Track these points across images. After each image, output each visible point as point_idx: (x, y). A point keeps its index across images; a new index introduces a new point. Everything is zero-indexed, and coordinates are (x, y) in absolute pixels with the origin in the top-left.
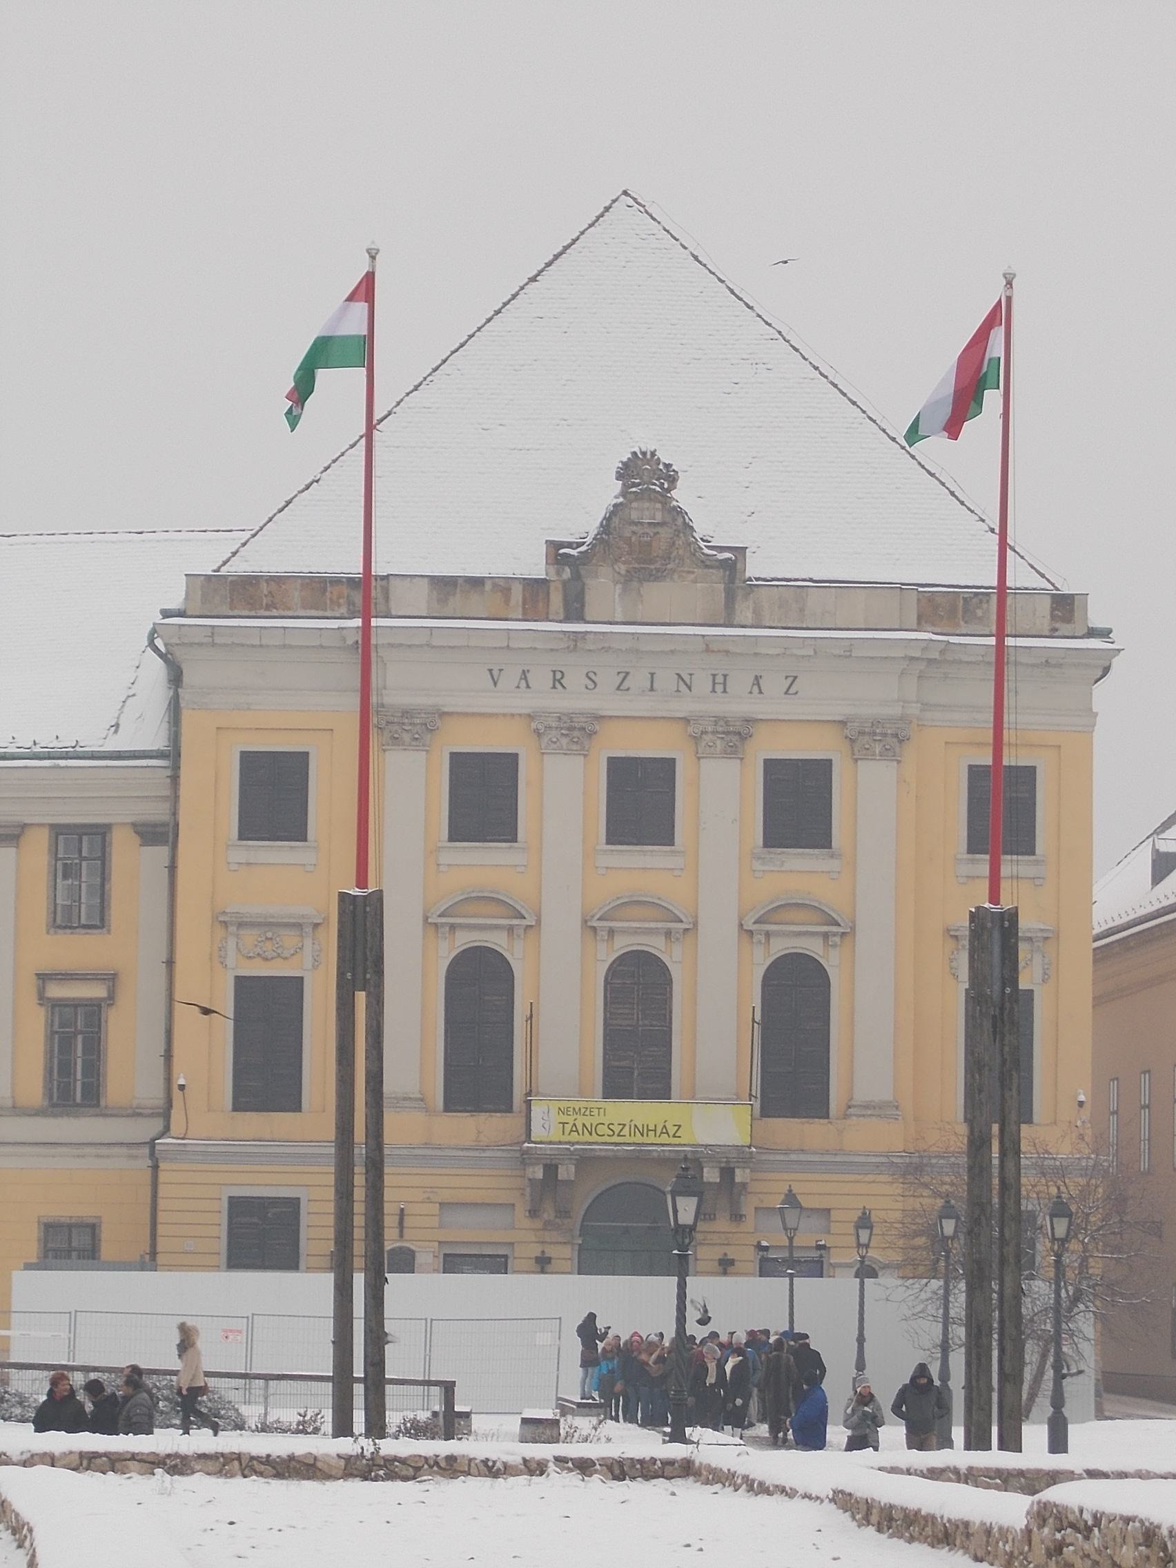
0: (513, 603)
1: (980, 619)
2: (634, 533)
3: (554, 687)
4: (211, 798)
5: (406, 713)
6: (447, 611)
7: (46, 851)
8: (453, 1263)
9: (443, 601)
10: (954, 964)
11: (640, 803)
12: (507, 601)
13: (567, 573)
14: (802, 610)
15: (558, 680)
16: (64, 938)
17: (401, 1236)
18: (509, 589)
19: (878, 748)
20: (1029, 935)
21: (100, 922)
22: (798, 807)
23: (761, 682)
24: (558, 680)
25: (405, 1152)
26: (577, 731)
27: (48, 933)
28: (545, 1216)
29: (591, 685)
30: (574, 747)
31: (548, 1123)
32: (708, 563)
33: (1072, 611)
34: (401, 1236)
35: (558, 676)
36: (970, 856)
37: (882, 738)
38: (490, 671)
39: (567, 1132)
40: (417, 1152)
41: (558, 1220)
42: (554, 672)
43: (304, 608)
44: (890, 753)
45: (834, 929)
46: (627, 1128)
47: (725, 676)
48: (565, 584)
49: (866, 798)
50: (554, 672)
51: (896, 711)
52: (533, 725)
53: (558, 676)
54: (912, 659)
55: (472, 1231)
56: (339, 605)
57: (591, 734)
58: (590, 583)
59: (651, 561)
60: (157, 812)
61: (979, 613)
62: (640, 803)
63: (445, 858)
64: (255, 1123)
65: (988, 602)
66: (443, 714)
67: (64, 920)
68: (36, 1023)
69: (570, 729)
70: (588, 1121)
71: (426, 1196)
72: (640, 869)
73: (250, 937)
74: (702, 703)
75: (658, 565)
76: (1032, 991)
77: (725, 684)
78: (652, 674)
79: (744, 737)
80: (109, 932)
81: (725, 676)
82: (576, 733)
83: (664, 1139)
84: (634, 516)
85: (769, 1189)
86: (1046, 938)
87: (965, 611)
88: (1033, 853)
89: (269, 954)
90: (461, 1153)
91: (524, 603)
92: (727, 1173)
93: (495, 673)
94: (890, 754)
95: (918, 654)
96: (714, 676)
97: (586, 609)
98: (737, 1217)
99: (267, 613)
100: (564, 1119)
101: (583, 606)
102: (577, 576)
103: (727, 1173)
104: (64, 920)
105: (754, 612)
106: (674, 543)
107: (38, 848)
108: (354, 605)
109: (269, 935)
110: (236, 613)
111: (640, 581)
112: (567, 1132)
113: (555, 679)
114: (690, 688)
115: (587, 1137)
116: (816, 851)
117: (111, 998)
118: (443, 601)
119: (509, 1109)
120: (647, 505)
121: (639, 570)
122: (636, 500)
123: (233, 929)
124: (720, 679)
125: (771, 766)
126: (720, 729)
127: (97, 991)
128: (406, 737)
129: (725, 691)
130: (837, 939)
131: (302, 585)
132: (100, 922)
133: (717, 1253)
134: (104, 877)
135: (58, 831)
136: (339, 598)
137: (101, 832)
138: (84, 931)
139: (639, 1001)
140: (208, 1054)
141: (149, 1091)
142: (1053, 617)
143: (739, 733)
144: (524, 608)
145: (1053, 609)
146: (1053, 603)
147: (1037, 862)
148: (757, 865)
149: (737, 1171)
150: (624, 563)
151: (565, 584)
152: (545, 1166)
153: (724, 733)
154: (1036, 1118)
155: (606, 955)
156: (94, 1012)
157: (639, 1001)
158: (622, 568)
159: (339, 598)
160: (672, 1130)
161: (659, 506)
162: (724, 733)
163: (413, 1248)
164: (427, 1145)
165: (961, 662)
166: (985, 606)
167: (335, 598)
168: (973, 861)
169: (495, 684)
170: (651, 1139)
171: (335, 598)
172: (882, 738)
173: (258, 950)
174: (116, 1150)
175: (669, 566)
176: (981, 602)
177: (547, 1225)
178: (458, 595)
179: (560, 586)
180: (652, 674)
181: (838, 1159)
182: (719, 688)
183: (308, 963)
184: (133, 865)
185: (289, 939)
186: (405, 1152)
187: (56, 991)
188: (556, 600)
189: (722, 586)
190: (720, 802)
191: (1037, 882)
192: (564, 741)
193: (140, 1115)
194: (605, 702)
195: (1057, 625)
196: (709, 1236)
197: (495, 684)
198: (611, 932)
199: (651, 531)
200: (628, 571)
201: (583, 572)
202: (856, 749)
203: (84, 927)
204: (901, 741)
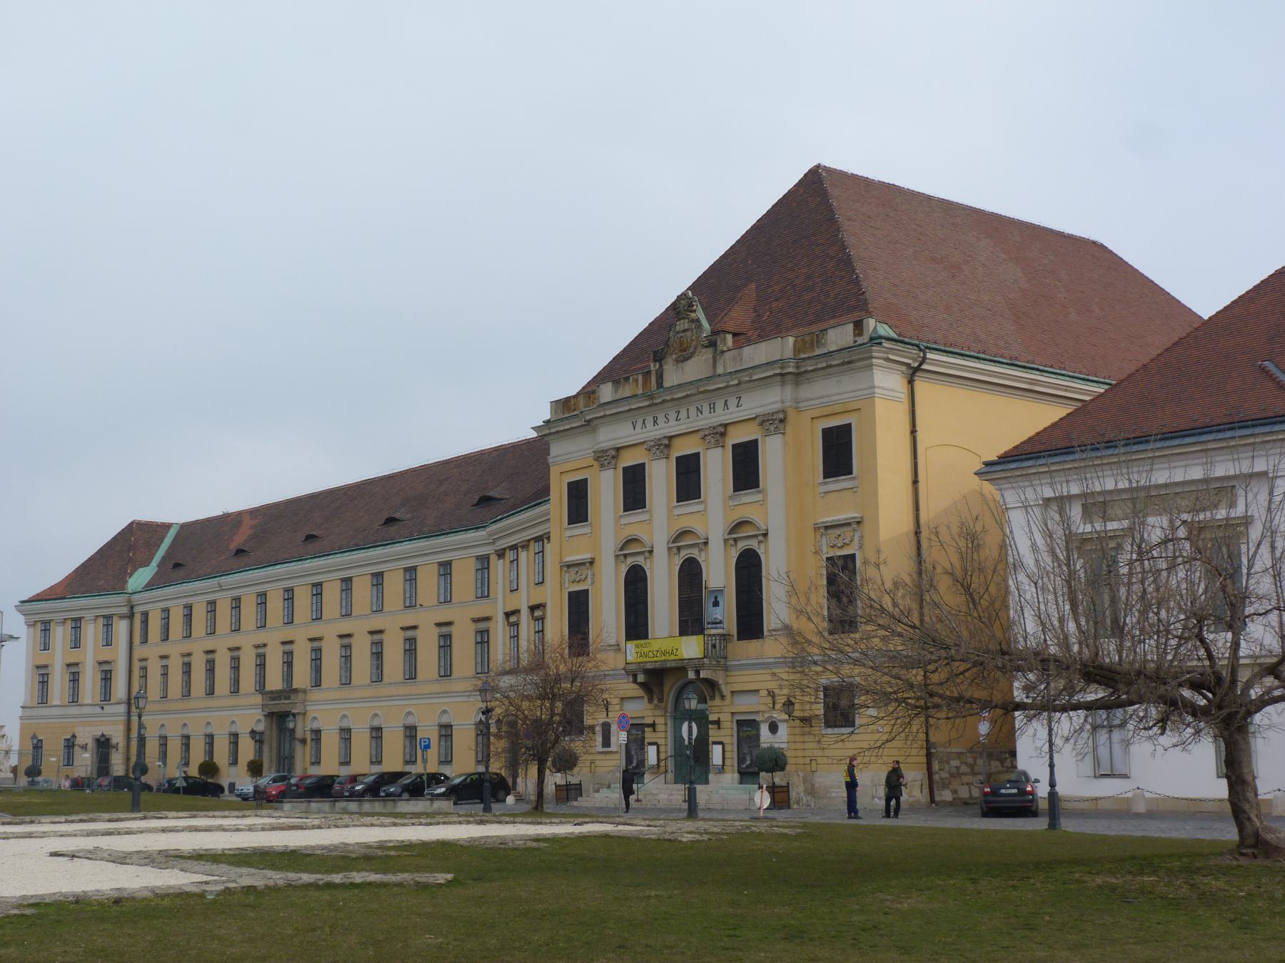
9: (616, 392)
11: (688, 480)
19: (772, 428)
37: (775, 422)
49: (772, 456)
51: (777, 406)
58: (665, 367)
62: (688, 480)
79: (723, 435)
95: (778, 371)
102: (661, 366)
118: (616, 392)
130: (761, 538)
142: (855, 335)
147: (853, 478)
148: (731, 503)
165: (806, 372)
172: (775, 422)
198: (679, 548)
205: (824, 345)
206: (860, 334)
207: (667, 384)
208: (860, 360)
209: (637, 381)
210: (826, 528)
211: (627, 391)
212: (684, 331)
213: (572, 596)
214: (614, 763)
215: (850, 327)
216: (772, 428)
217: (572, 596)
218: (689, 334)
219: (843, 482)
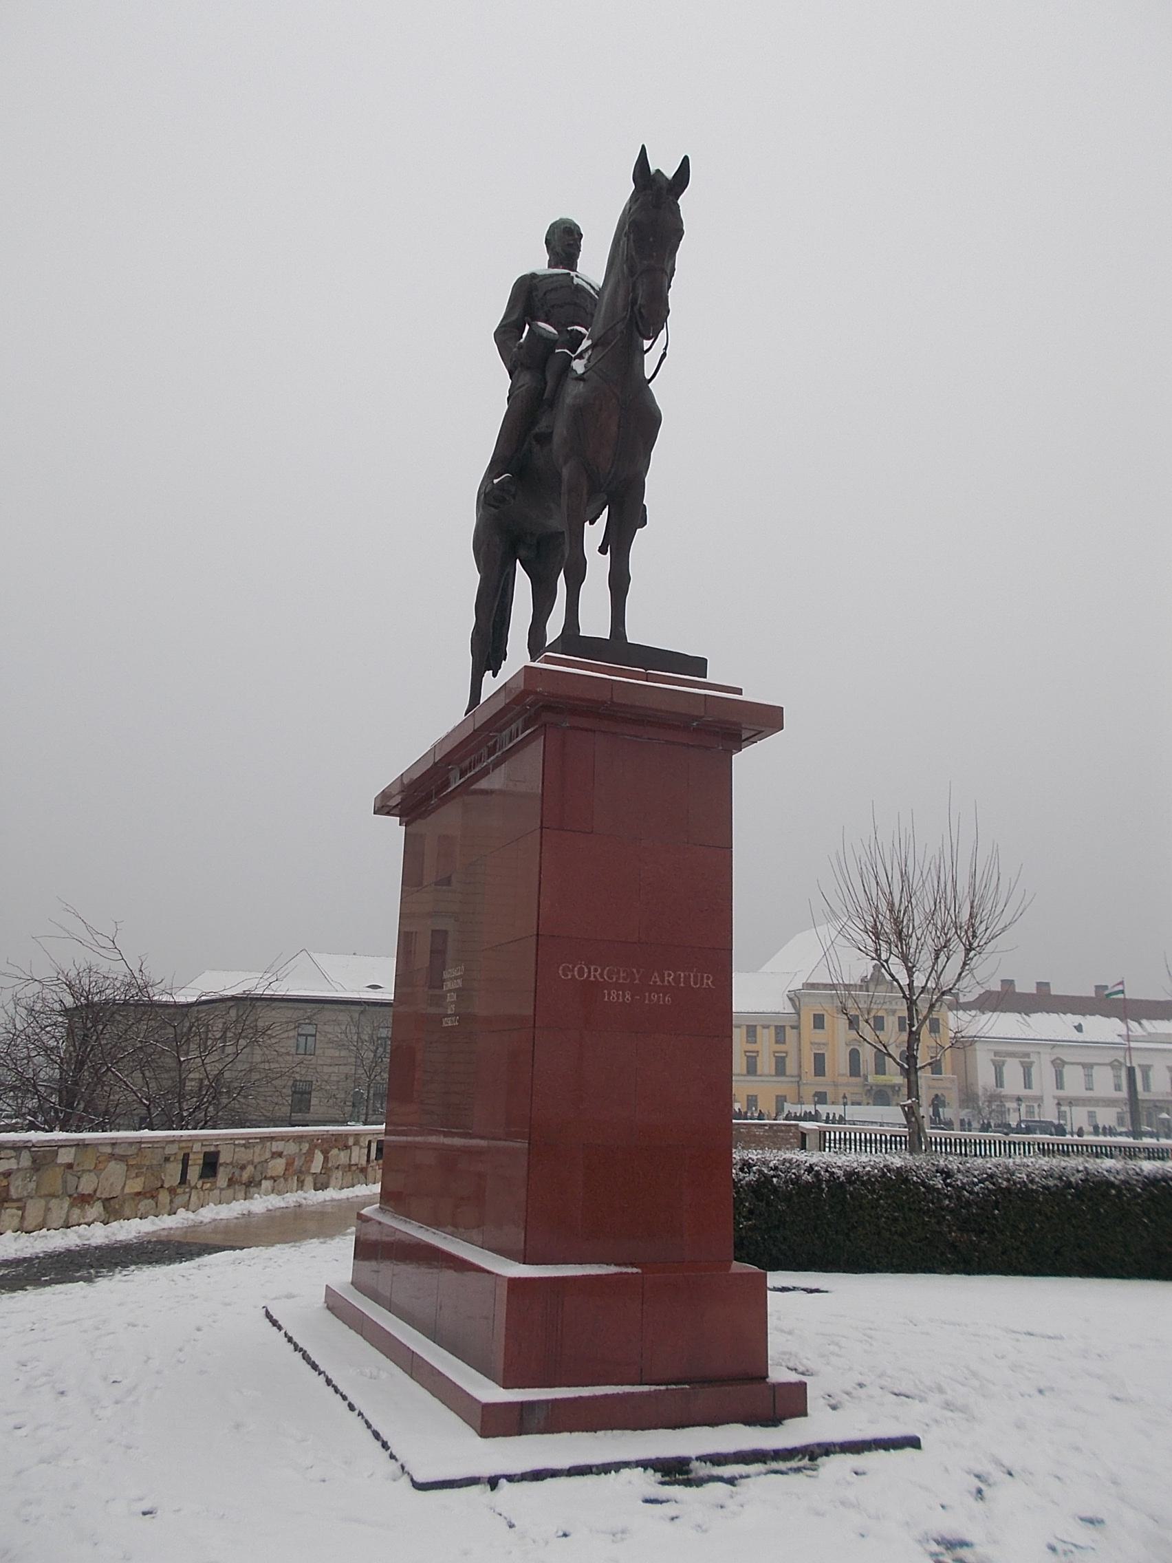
4: (807, 1021)
8: (853, 1104)
21: (784, 1043)
31: (870, 1079)
55: (857, 1098)
67: (777, 1042)
68: (773, 1060)
104: (777, 1042)
107: (773, 1029)
132: (784, 1043)
135: (776, 1027)
137: (784, 1027)
140: (809, 1066)
141: (795, 1072)
156: (783, 1058)
184: (790, 1034)
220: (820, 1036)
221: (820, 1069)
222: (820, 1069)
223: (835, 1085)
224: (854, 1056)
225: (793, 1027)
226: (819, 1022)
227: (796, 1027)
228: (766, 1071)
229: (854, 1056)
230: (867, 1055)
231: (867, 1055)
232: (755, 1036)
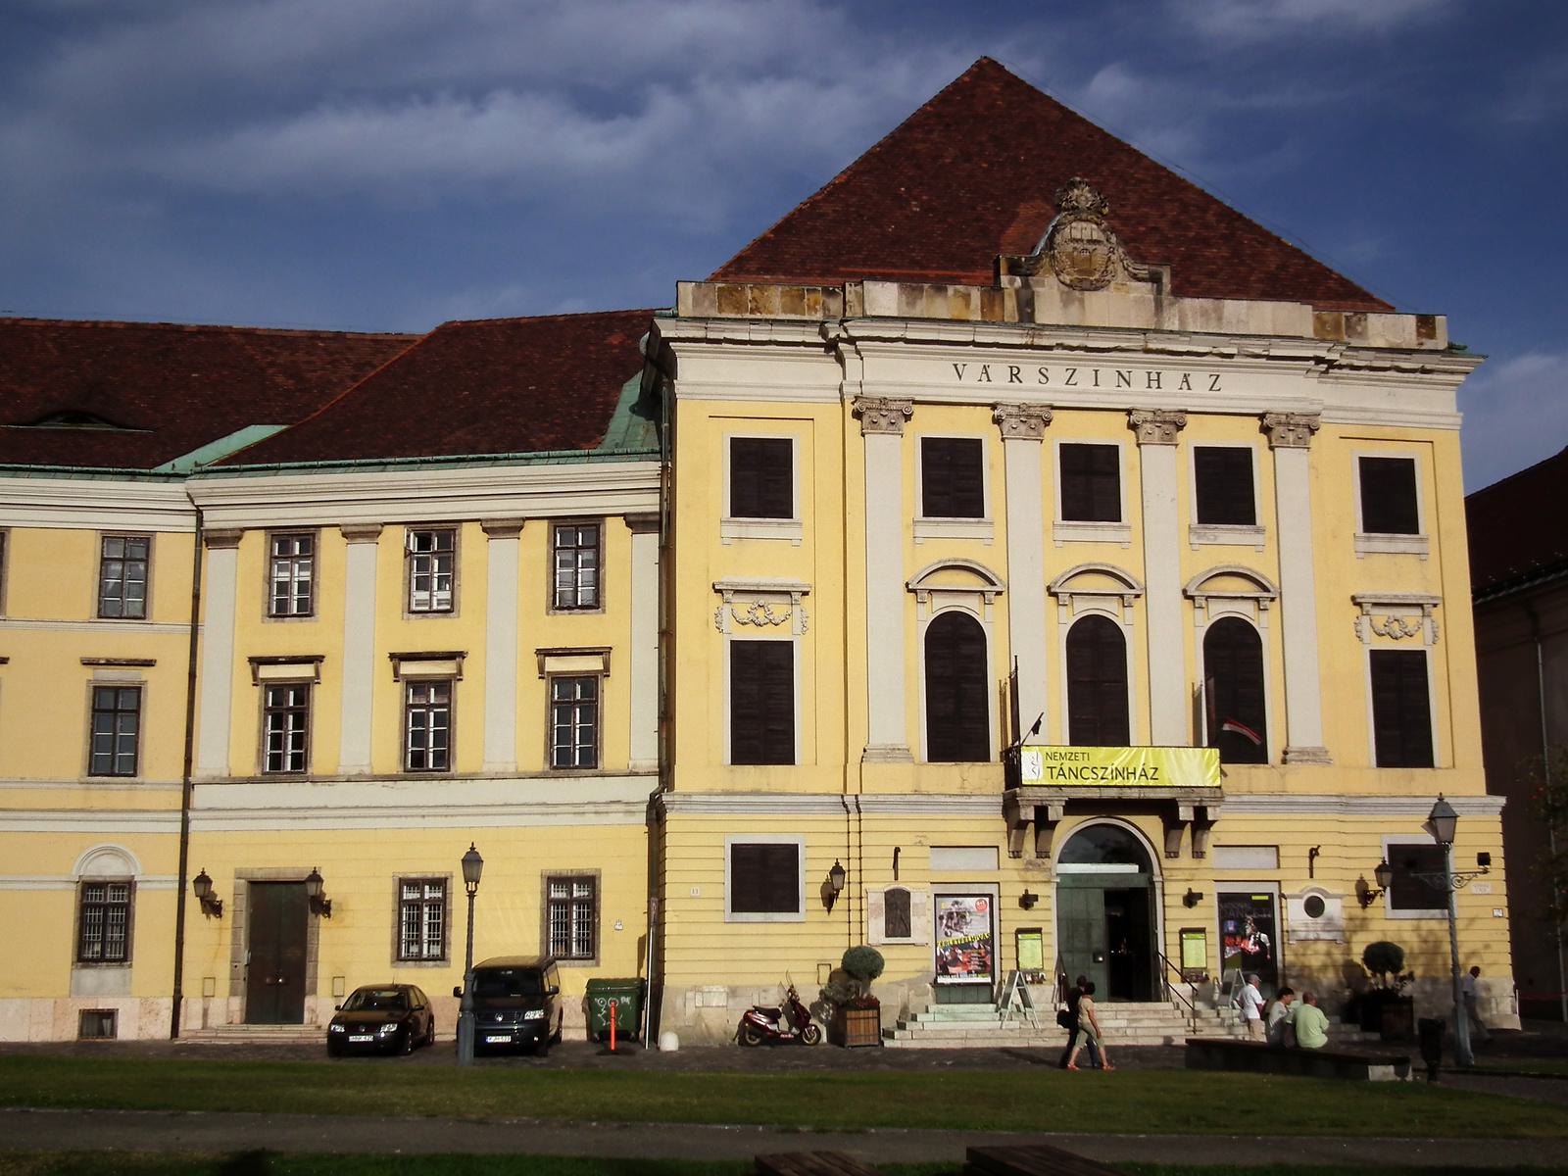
0: (972, 307)
1: (1360, 334)
2: (1075, 248)
3: (1012, 381)
5: (884, 401)
6: (916, 313)
7: (545, 542)
9: (911, 303)
10: (1359, 628)
11: (1090, 485)
12: (968, 304)
13: (1018, 281)
14: (1220, 319)
15: (1015, 376)
16: (563, 617)
17: (896, 879)
18: (969, 295)
20: (1421, 602)
21: (596, 604)
22: (1225, 488)
23: (1189, 378)
24: (1015, 376)
25: (898, 798)
26: (1037, 418)
27: (548, 614)
28: (1027, 856)
29: (1044, 380)
30: (1032, 433)
32: (1140, 276)
33: (1434, 328)
34: (896, 879)
35: (1015, 371)
36: (1367, 535)
38: (955, 365)
39: (1055, 774)
40: (907, 798)
41: (1039, 861)
42: (1011, 367)
43: (784, 312)
44: (1301, 441)
45: (1266, 594)
46: (1109, 771)
47: (1159, 374)
48: (1017, 291)
50: (1011, 367)
52: (996, 412)
53: (1015, 371)
54: (1319, 360)
56: (816, 311)
57: (1047, 423)
58: (1037, 289)
59: (1091, 273)
60: (649, 503)
61: (1359, 329)
62: (1090, 485)
63: (922, 531)
64: (754, 776)
65: (1366, 320)
66: (915, 402)
69: (1030, 416)
70: (1073, 765)
71: (919, 839)
72: (1093, 541)
73: (743, 606)
74: (1139, 395)
75: (1097, 276)
76: (1424, 652)
77: (1158, 380)
78: (1096, 371)
80: (604, 611)
81: (1159, 374)
82: (1033, 421)
83: (1143, 782)
84: (1077, 234)
85: (1227, 824)
86: (1435, 605)
87: (1348, 327)
88: (1417, 532)
89: (762, 620)
90: (948, 799)
91: (982, 308)
92: (1200, 812)
93: (960, 367)
94: (1302, 444)
95: (1322, 353)
96: (1149, 373)
97: (1036, 313)
98: (1198, 854)
99: (752, 316)
100: (1052, 763)
101: (1033, 311)
102: (1026, 285)
103: (1200, 812)
104: (561, 603)
105: (1179, 320)
106: (1109, 258)
108: (829, 310)
109: (762, 602)
110: (724, 315)
111: (1083, 290)
112: (1055, 774)
113: (1012, 374)
114: (1129, 384)
115: (1073, 781)
116: (1245, 527)
117: (606, 671)
118: (911, 303)
119: (986, 758)
120: (1084, 225)
121: (1081, 281)
122: (1075, 221)
123: (728, 596)
124: (1154, 376)
125: (1201, 453)
126: (1158, 419)
127: (594, 664)
128: (883, 422)
129: (1159, 387)
131: (782, 292)
132: (596, 604)
133: (1182, 889)
134: (597, 564)
135: (557, 523)
136: (816, 303)
138: (581, 611)
139: (1097, 662)
141: (647, 755)
142: (1419, 334)
143: (1175, 423)
144: (982, 312)
145: (1418, 328)
146: (1418, 322)
148: (1194, 539)
149: (1209, 809)
150: (1068, 274)
151: (1017, 291)
152: (1036, 807)
153: (1161, 422)
154: (1436, 762)
155: (1069, 617)
156: (590, 683)
157: (1097, 662)
158: (1067, 279)
159: (816, 303)
160: (1150, 773)
161: (1094, 226)
162: (1161, 422)
163: (908, 889)
164: (917, 793)
166: (1363, 323)
167: (812, 304)
168: (1369, 539)
169: (960, 377)
170: (1132, 782)
171: (812, 304)
173: (751, 617)
174: (614, 807)
175: (1107, 278)
176: (1360, 320)
177: (1030, 866)
178: (924, 299)
179: (1014, 294)
180: (1096, 371)
181: (1284, 799)
182: (1154, 384)
183: (798, 628)
185: (778, 607)
186: (898, 798)
187: (553, 665)
188: (1010, 304)
189: (1152, 297)
190: (1159, 483)
191: (1423, 557)
192: (1023, 428)
193: (637, 774)
194: (1055, 391)
195: (1424, 340)
196: (1174, 872)
197: (960, 377)
199: (1091, 247)
200: (1071, 281)
201: (1031, 282)
202: (1273, 440)
203: (583, 607)
204: (1312, 431)
205: (1361, 335)
206: (1431, 335)
207: (1041, 317)
208: (1445, 372)
209: (967, 297)
210: (1375, 604)
211: (941, 306)
212: (1091, 241)
213: (742, 653)
214: (920, 965)
215: (1410, 322)
216: (1291, 437)
217: (742, 653)
218: (1102, 250)
219: (1402, 542)
220: (765, 551)
221: (763, 724)
222: (763, 724)
223: (851, 806)
224: (955, 653)
225: (637, 523)
226: (762, 479)
227: (660, 523)
228: (498, 759)
229: (955, 653)
230: (1030, 660)
231: (1030, 660)
232: (448, 578)
